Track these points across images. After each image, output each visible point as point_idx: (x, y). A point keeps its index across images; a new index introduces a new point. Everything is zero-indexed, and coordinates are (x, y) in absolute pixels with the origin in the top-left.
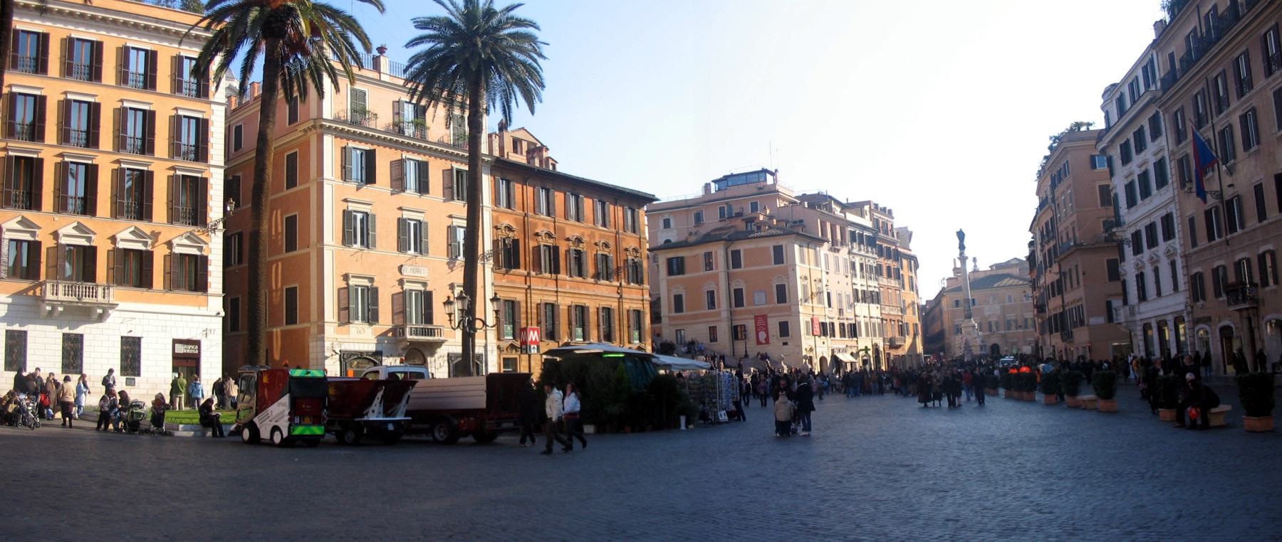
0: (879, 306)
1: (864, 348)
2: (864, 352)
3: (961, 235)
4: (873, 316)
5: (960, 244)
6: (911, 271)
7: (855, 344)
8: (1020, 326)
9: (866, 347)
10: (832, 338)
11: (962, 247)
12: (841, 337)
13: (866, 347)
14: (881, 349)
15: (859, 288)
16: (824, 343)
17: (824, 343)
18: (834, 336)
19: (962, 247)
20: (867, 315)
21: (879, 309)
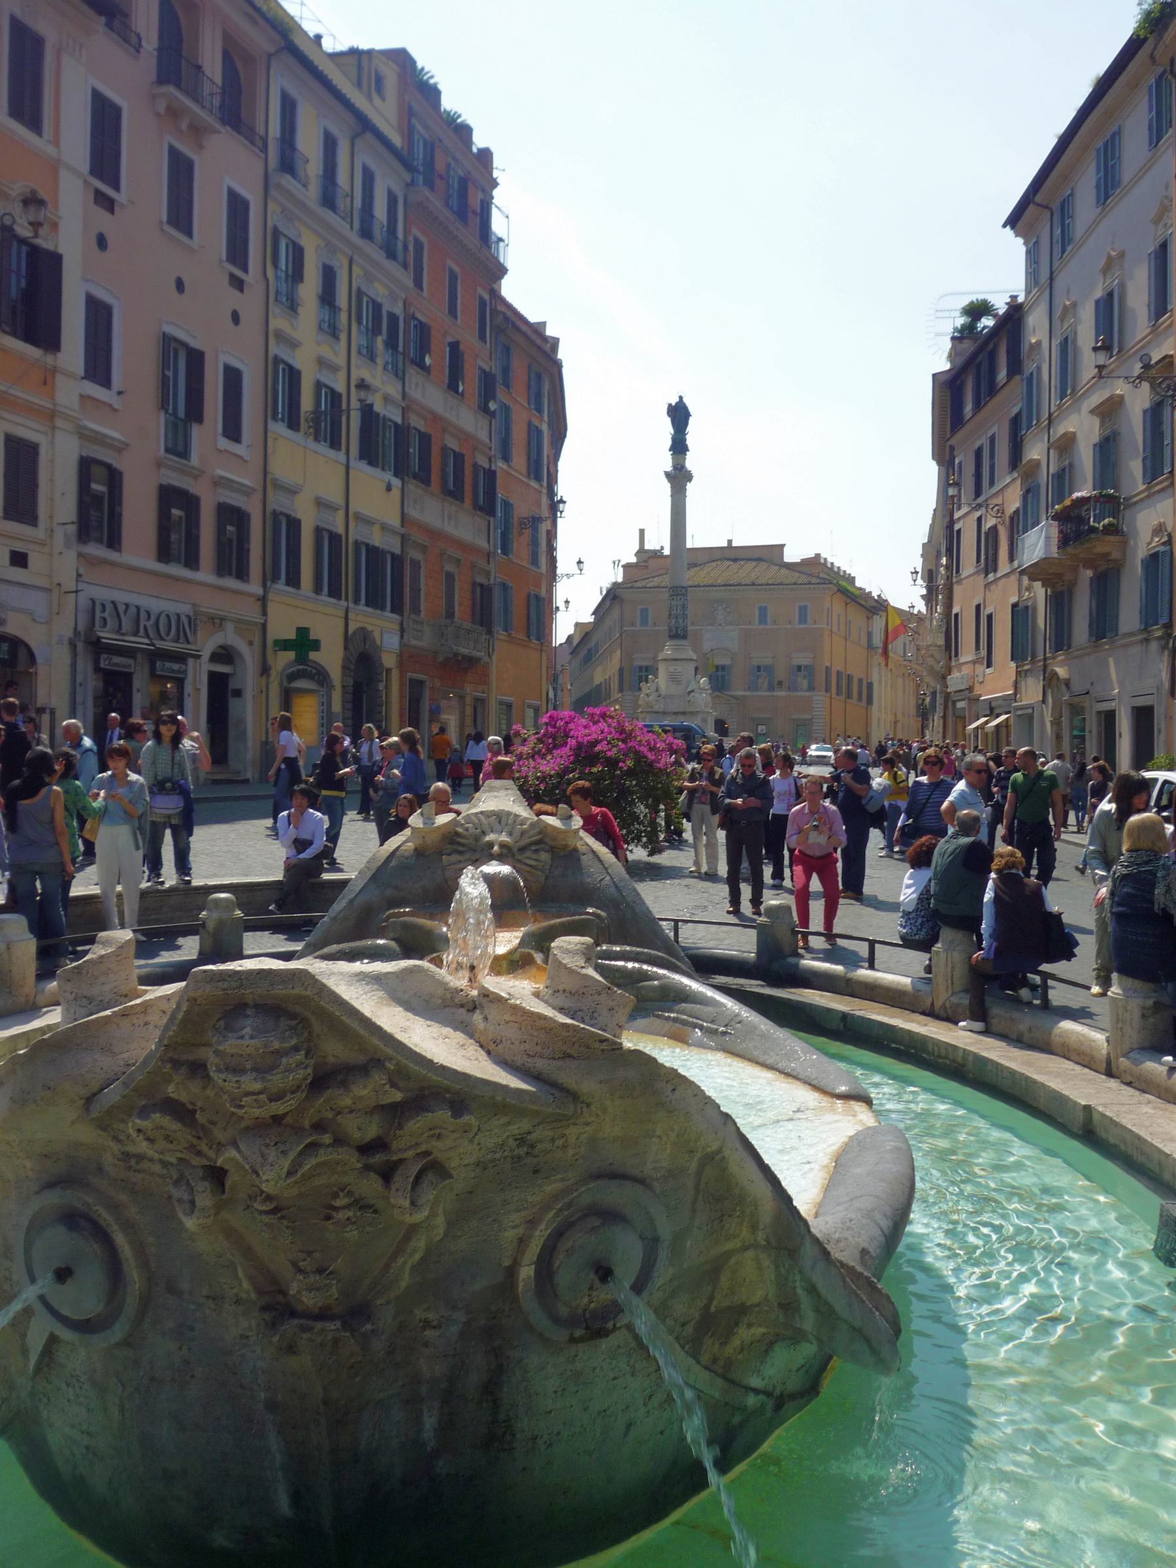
0: (396, 482)
1: (292, 635)
2: (291, 655)
3: (679, 414)
4: (367, 511)
5: (674, 440)
6: (539, 409)
7: (252, 613)
8: (780, 683)
9: (303, 632)
10: (96, 550)
11: (679, 447)
12: (164, 553)
13: (303, 632)
14: (389, 660)
15: (303, 360)
16: (19, 559)
17: (19, 559)
18: (114, 541)
19: (679, 447)
20: (337, 498)
21: (396, 493)
